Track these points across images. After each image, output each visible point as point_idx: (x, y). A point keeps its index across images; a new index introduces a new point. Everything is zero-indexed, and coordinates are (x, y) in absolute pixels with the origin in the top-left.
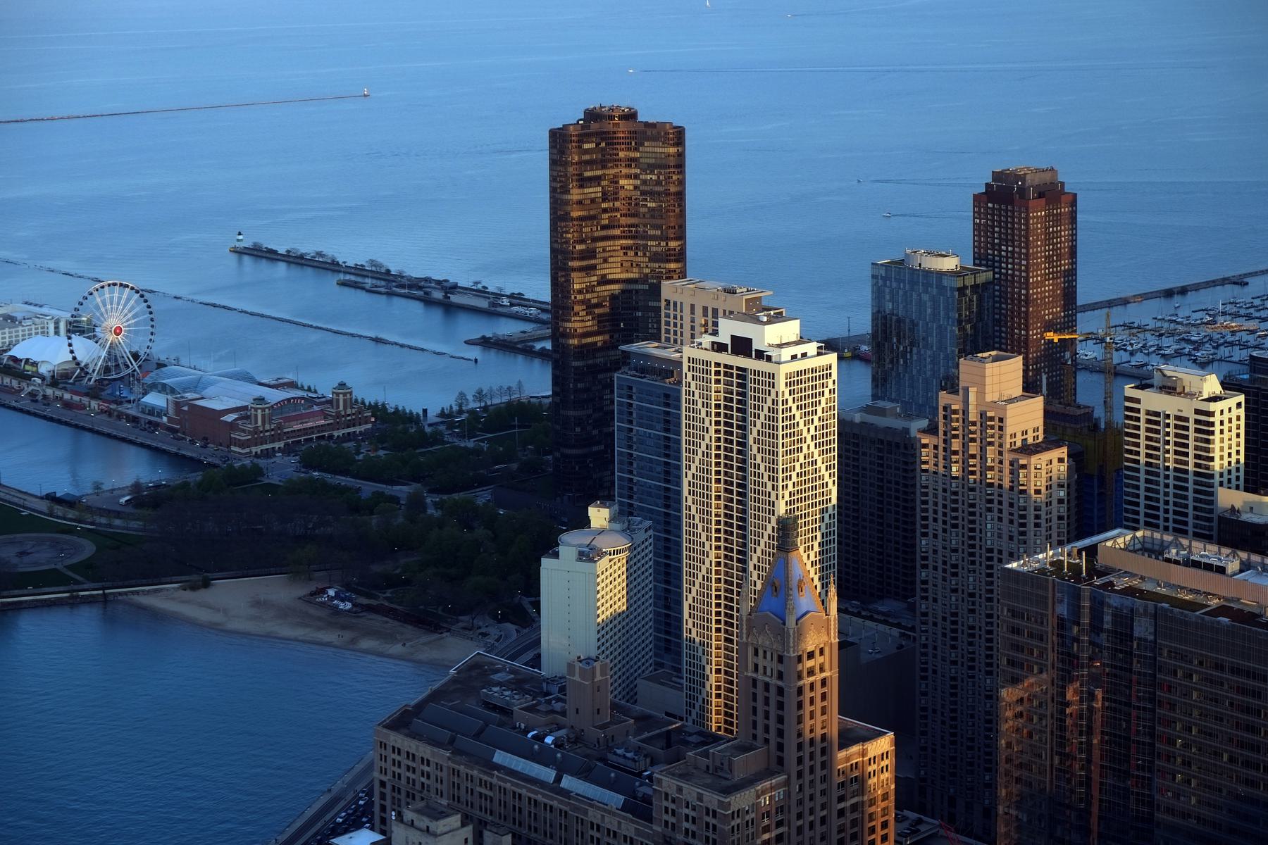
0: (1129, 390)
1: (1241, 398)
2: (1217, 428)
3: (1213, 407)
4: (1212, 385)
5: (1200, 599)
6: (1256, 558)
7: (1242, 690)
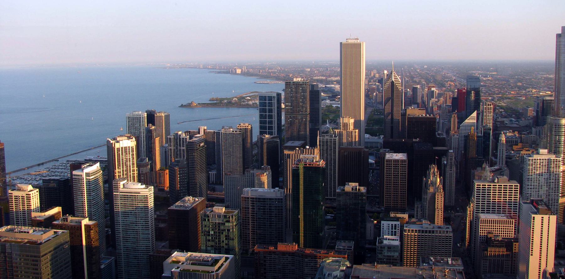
0: (10, 191)
1: (38, 190)
2: (32, 198)
3: (31, 193)
4: (30, 187)
5: (23, 240)
6: (37, 228)
7: (33, 261)
